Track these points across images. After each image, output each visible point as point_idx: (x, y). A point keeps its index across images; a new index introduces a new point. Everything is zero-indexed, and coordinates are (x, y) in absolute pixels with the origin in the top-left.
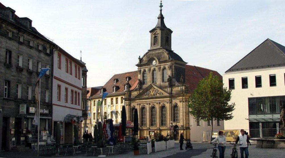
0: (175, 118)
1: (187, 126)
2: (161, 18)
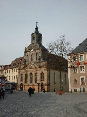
0: (42, 80)
1: (48, 84)
2: (37, 28)
